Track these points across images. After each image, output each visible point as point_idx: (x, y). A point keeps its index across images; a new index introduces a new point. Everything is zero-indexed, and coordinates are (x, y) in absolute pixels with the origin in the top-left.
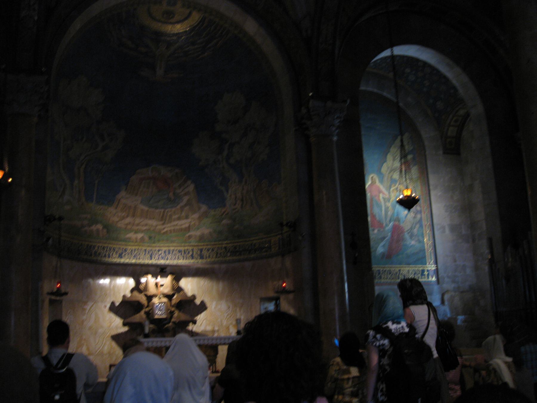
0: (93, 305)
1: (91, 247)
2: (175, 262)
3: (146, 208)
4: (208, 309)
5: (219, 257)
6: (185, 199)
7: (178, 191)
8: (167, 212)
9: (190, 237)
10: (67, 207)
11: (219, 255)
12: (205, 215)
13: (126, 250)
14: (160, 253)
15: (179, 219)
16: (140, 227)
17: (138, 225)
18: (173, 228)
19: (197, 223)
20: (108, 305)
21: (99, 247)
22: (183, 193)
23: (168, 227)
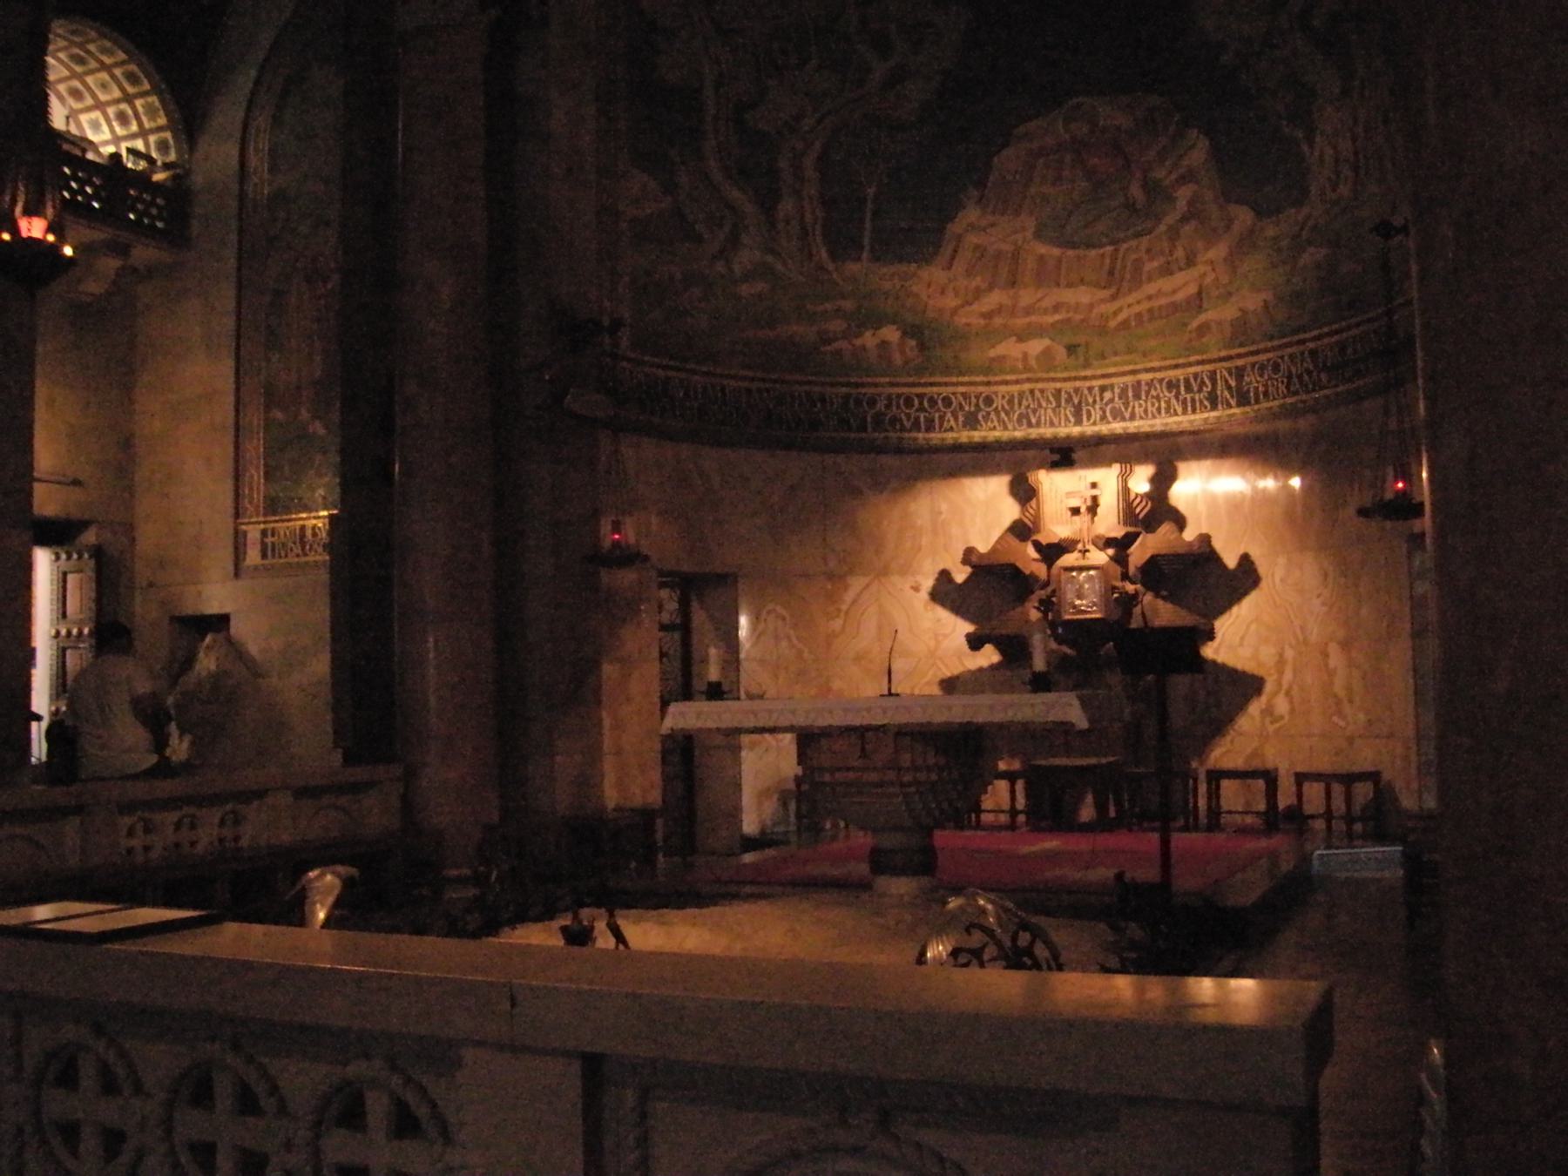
0: (867, 586)
1: (858, 402)
2: (1158, 423)
3: (1056, 251)
4: (1263, 584)
5: (1296, 393)
6: (1184, 194)
7: (1159, 174)
8: (1128, 249)
9: (1203, 329)
10: (760, 286)
11: (1296, 386)
12: (1246, 244)
13: (989, 401)
14: (1107, 395)
15: (1167, 271)
16: (1033, 318)
17: (1029, 311)
18: (1145, 306)
19: (1225, 279)
20: (928, 583)
21: (889, 397)
22: (1173, 176)
23: (1129, 306)
